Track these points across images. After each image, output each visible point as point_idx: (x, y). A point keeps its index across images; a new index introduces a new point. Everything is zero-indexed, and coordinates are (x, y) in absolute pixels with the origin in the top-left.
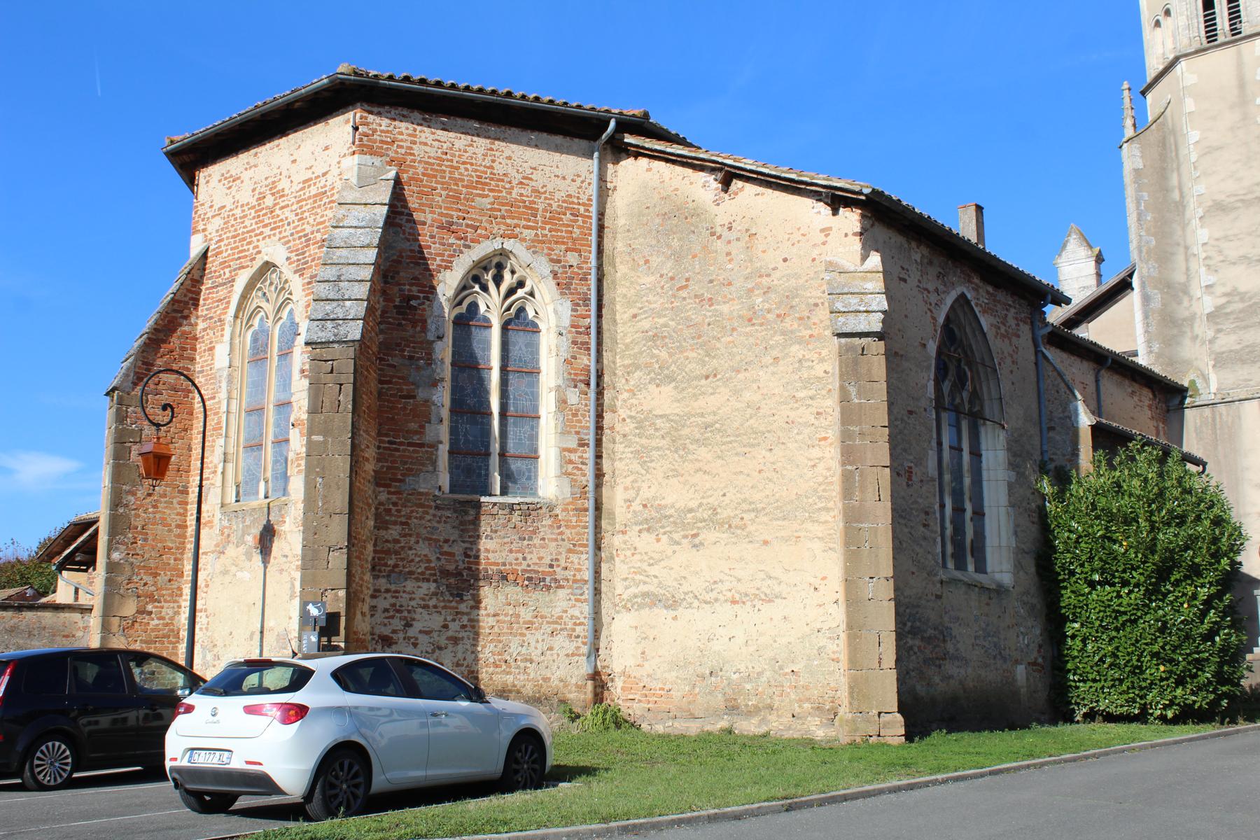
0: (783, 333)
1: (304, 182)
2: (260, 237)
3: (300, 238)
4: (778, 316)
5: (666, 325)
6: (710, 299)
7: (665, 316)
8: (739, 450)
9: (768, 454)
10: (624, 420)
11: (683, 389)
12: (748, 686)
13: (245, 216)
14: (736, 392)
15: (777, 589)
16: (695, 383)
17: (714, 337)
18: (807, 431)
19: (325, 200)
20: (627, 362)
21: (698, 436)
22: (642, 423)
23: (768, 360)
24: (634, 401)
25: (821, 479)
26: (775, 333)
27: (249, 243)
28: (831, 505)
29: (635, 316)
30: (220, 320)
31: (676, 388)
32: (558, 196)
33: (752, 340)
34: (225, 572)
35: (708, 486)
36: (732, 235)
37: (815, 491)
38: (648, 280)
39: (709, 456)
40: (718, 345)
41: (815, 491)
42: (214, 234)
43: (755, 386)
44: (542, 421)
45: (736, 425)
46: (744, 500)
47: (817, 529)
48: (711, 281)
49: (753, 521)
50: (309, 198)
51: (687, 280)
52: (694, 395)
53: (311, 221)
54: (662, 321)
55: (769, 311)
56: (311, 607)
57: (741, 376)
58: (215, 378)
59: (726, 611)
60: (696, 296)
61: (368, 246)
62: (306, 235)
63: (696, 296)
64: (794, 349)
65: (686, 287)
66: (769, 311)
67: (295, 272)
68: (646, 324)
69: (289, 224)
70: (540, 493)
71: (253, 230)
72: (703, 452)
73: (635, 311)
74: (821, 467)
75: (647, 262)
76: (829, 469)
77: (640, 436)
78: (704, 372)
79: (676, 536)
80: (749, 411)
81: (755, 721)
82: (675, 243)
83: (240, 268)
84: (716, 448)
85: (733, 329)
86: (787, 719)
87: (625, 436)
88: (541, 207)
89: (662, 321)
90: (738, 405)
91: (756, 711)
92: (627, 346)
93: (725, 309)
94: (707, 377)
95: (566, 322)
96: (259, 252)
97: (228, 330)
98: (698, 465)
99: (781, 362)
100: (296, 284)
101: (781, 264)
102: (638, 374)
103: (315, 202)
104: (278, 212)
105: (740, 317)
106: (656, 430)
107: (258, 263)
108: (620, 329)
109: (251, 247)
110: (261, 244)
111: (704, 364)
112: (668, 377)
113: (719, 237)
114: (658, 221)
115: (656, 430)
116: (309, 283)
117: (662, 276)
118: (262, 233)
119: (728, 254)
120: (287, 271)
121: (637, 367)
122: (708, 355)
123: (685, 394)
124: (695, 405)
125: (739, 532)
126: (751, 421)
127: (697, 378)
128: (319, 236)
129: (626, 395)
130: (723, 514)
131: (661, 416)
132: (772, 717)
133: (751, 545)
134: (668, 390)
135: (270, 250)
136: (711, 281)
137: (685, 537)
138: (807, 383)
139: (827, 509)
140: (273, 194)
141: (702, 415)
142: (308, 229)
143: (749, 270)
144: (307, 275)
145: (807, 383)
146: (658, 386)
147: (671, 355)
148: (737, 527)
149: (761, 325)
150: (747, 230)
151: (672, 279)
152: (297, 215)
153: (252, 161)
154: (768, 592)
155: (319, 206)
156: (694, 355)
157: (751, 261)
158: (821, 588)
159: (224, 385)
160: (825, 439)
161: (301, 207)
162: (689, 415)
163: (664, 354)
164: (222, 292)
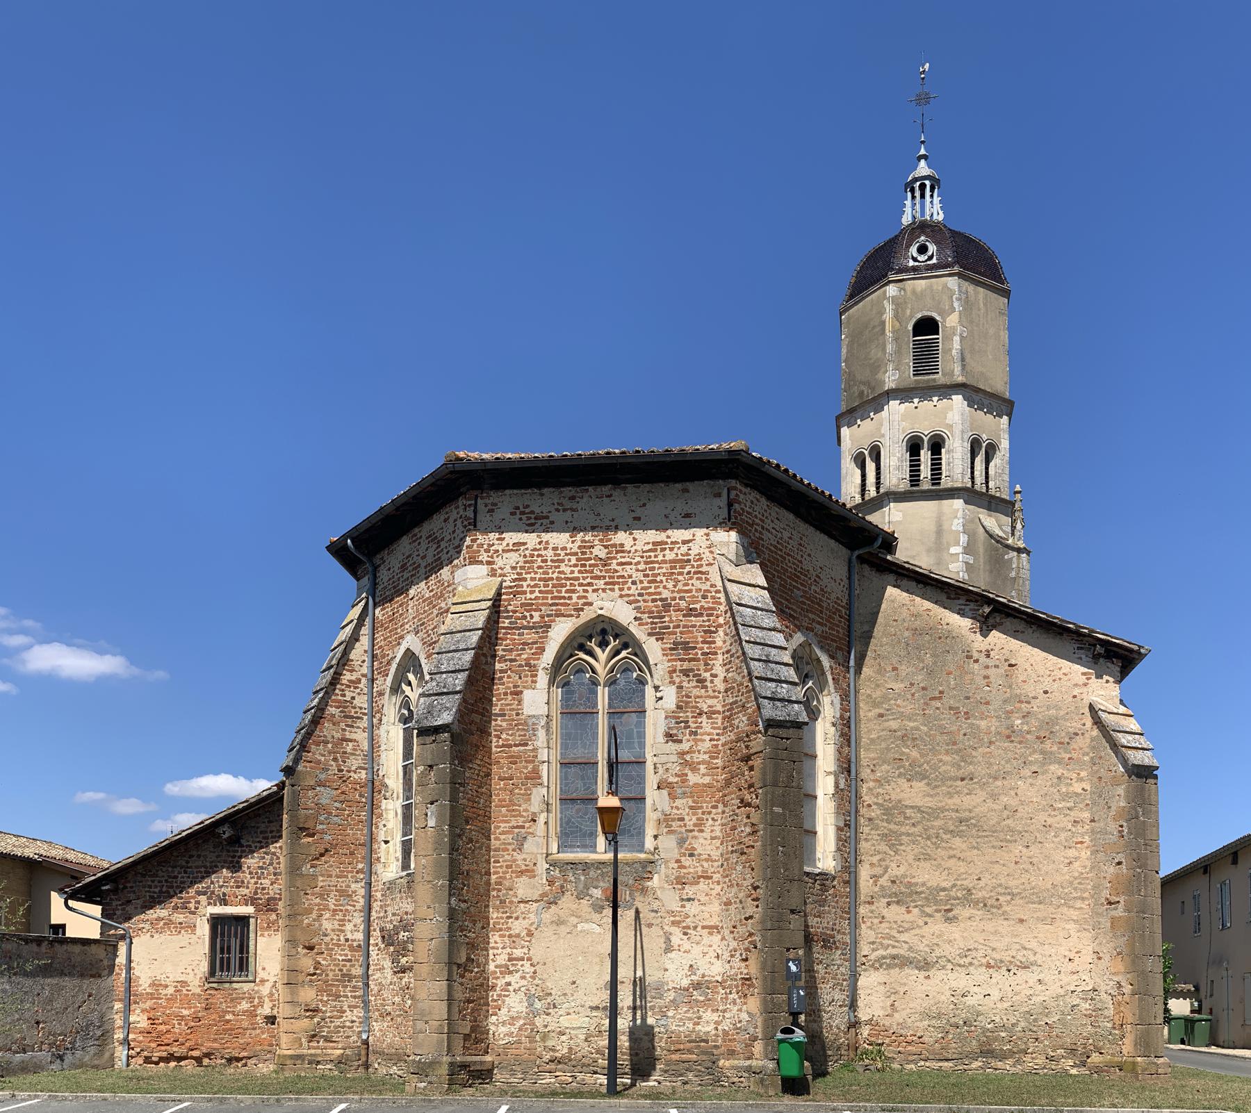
0: (1043, 752)
1: (654, 544)
2: (590, 589)
3: (654, 601)
4: (1038, 738)
5: (917, 729)
6: (966, 713)
7: (915, 721)
8: (996, 844)
9: (1025, 850)
10: (869, 806)
11: (936, 787)
12: (1003, 1034)
13: (563, 561)
14: (994, 797)
15: (1032, 958)
16: (949, 783)
17: (970, 747)
18: (1063, 835)
19: (688, 569)
20: (872, 755)
21: (952, 828)
22: (893, 810)
23: (1026, 772)
24: (880, 790)
25: (1076, 874)
26: (1035, 751)
27: (573, 591)
28: (1086, 895)
29: (881, 715)
30: (528, 665)
31: (928, 784)
32: (833, 596)
33: (1010, 755)
34: (560, 922)
35: (962, 870)
36: (990, 662)
37: (1071, 883)
38: (898, 686)
39: (964, 846)
40: (974, 753)
41: (1071, 883)
42: (508, 569)
43: (1013, 793)
44: (821, 800)
45: (992, 823)
46: (1000, 885)
47: (1074, 914)
48: (968, 698)
49: (1009, 902)
50: (664, 562)
51: (941, 692)
52: (949, 793)
53: (670, 585)
54: (912, 724)
55: (1029, 732)
56: (791, 964)
57: (999, 783)
58: (526, 723)
59: (980, 974)
60: (951, 708)
61: (774, 629)
62: (661, 600)
63: (951, 708)
64: (1052, 767)
65: (940, 698)
66: (1029, 732)
67: (650, 634)
68: (894, 725)
69: (634, 583)
70: (820, 865)
71: (577, 579)
72: (957, 842)
73: (882, 711)
74: (1076, 864)
75: (895, 669)
76: (1085, 867)
77: (888, 821)
78: (960, 774)
79: (928, 910)
80: (1006, 813)
81: (1010, 1062)
82: (928, 659)
83: (557, 615)
84: (971, 840)
85: (991, 743)
86: (1041, 1060)
87: (870, 820)
88: (825, 605)
89: (912, 724)
90: (996, 807)
91: (1012, 1053)
92: (872, 741)
93: (983, 724)
94: (962, 779)
95: (838, 715)
96: (591, 604)
97: (543, 679)
98: (952, 853)
99: (1040, 777)
100: (653, 649)
101: (1042, 696)
102: (885, 767)
103: (672, 568)
104: (614, 566)
105: (999, 733)
106: (906, 818)
107: (588, 615)
108: (863, 727)
109: (574, 596)
110: (592, 597)
111: (959, 767)
112: (917, 773)
113: (976, 661)
114: (907, 634)
115: (906, 818)
116: (671, 649)
117: (912, 684)
118: (589, 584)
119: (986, 677)
120: (639, 632)
121: (884, 762)
122: (965, 761)
123: (938, 790)
124: (950, 802)
125: (994, 910)
126: (1008, 822)
127: (951, 779)
128: (683, 604)
129: (871, 784)
130: (979, 895)
131: (912, 807)
132: (1028, 1058)
133: (1005, 923)
134: (920, 785)
135: (607, 604)
136: (968, 698)
137: (938, 911)
138: (1066, 796)
139: (1083, 899)
140: (606, 547)
141: (957, 811)
142: (666, 594)
143: (1008, 695)
144: (669, 641)
145: (1066, 796)
146: (909, 780)
147: (922, 755)
148: (992, 906)
149: (1020, 742)
150: (1006, 660)
151: (924, 689)
152: (645, 576)
153: (568, 504)
154: (1024, 960)
155: (681, 574)
156: (947, 758)
157: (1010, 687)
158: (1077, 959)
159: (541, 733)
160: (1082, 843)
161: (652, 569)
162: (943, 810)
163: (915, 754)
164: (529, 636)
